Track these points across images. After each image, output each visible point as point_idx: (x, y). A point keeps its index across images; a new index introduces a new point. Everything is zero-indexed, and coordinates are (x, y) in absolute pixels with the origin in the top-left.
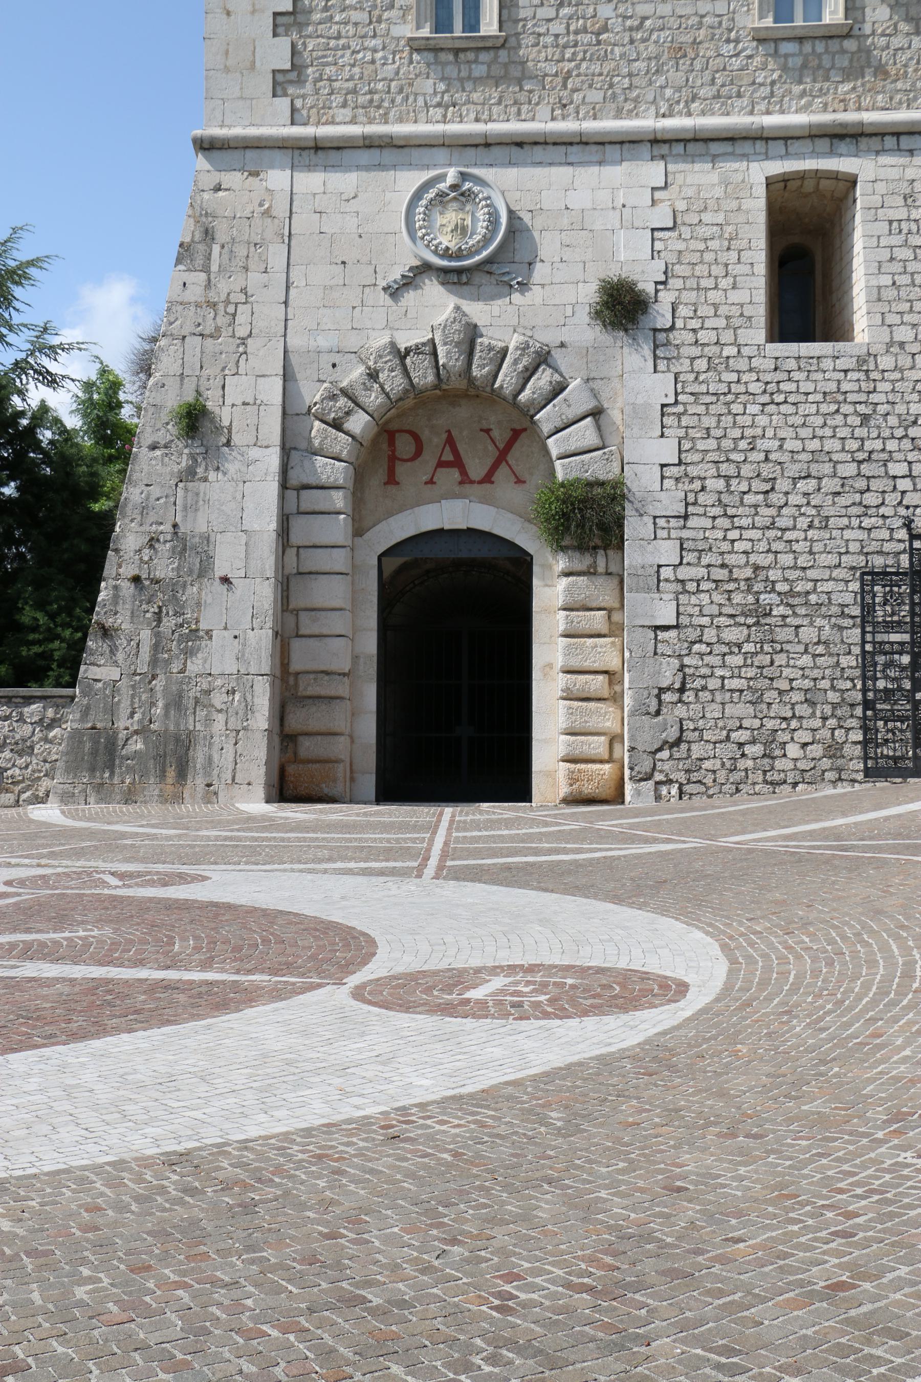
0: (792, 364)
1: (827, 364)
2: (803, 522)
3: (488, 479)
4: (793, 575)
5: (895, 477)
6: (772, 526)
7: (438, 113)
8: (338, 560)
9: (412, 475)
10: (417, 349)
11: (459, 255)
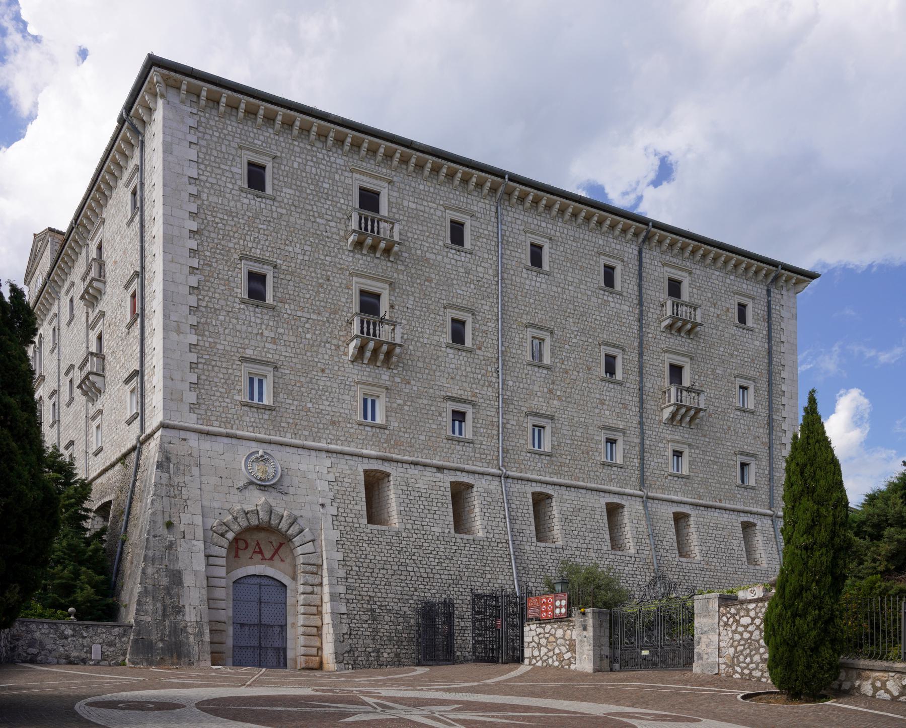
0: (376, 532)
1: (387, 533)
2: (383, 583)
3: (271, 559)
4: (382, 600)
6: (374, 584)
7: (251, 429)
8: (223, 583)
9: (245, 555)
10: (252, 512)
11: (265, 480)
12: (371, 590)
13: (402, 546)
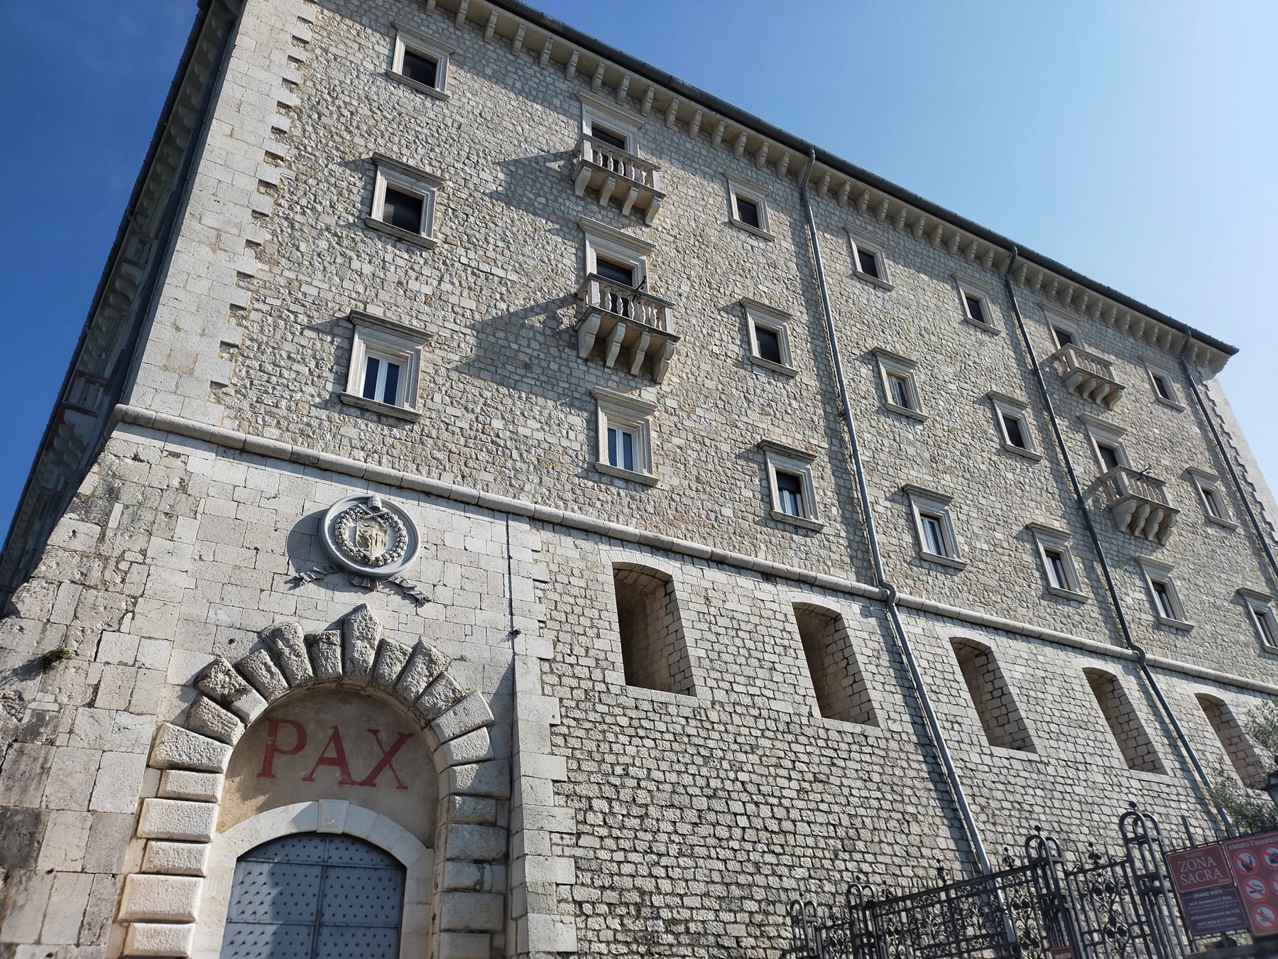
2: (674, 849)
3: (369, 781)
5: (735, 814)
12: (643, 870)
13: (711, 744)
